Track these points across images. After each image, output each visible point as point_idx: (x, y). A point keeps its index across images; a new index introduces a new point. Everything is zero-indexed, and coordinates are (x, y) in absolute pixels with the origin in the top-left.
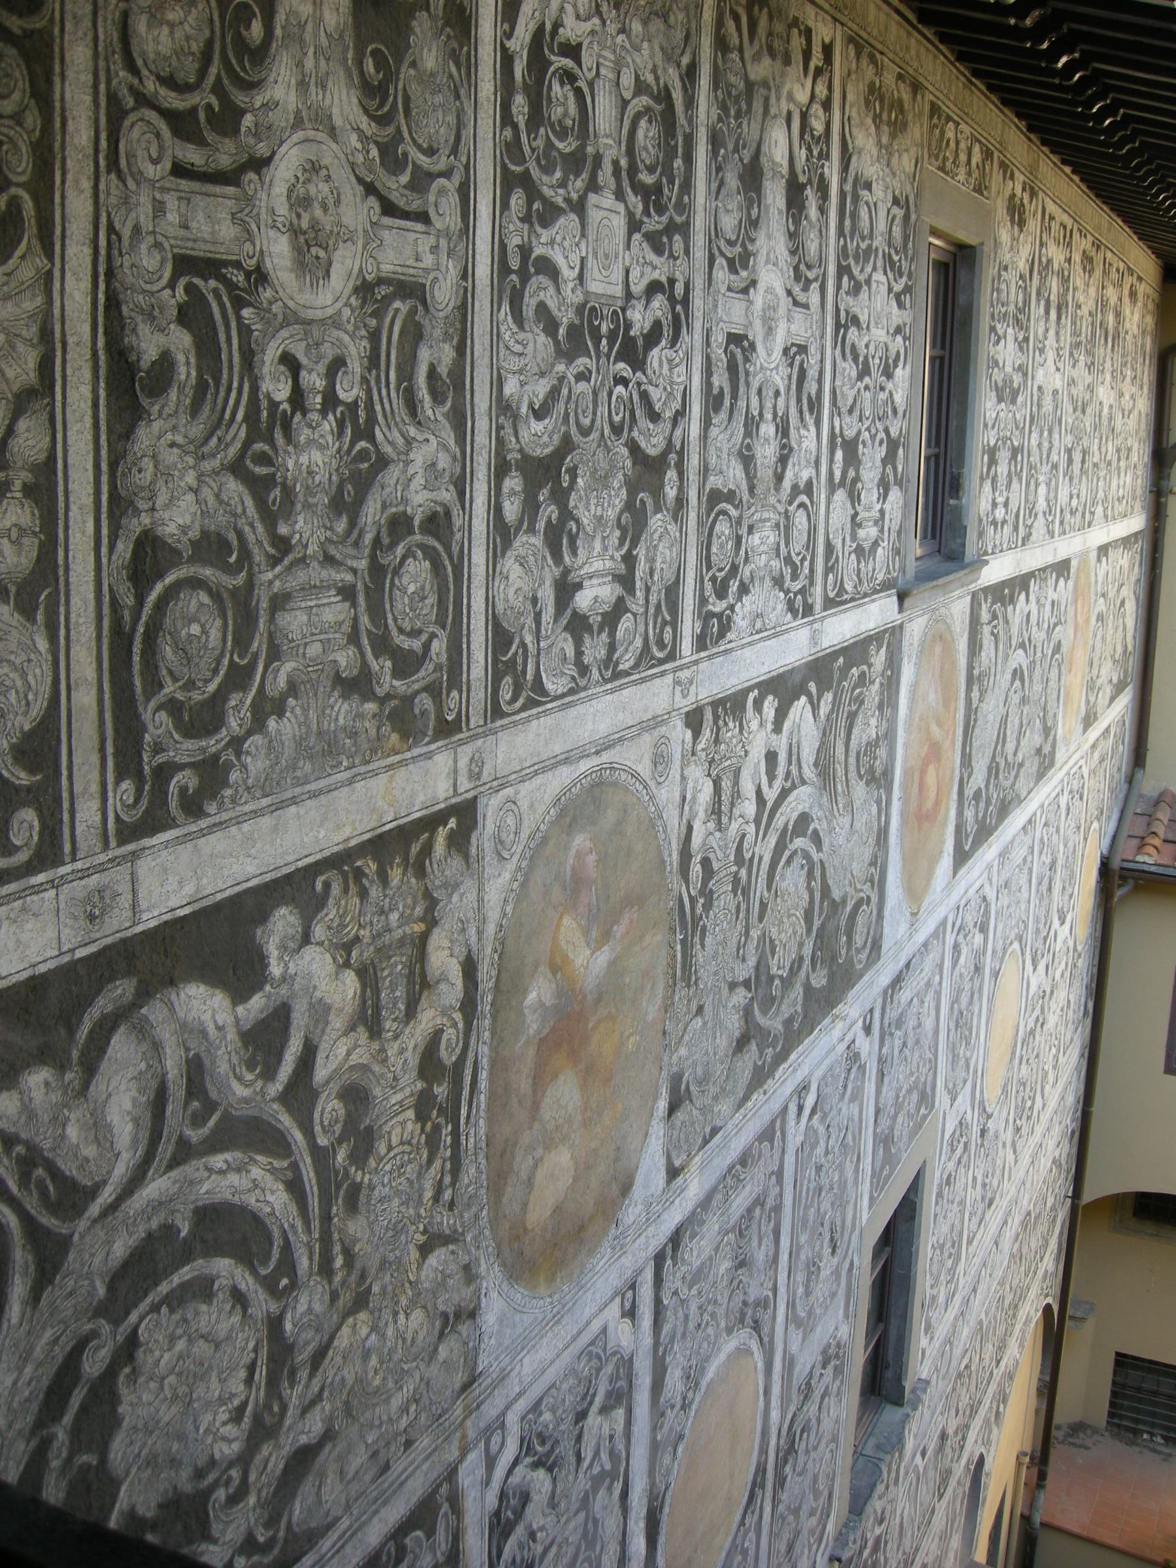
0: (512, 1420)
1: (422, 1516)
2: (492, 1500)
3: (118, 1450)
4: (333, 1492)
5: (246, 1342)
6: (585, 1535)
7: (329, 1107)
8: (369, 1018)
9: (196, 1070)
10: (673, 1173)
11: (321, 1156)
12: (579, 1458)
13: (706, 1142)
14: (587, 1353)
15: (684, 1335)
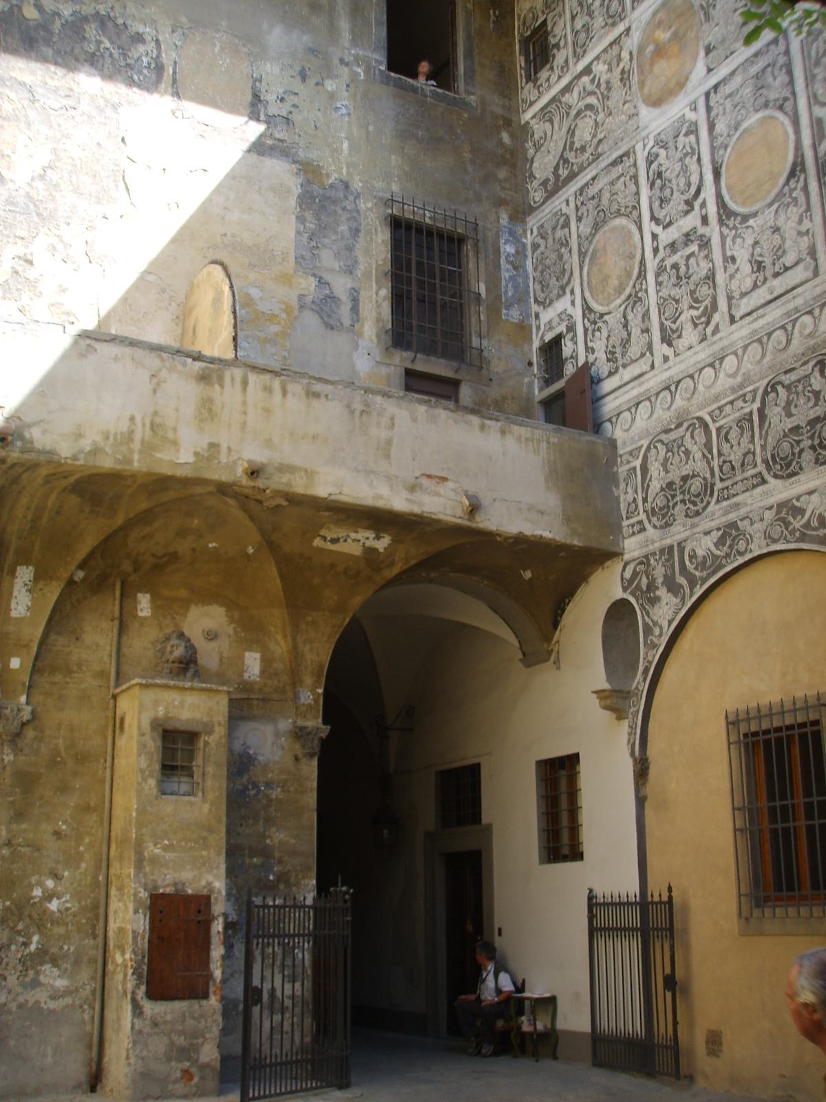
0: (651, 137)
1: (627, 154)
3: (576, 139)
5: (591, 123)
6: (682, 168)
7: (603, 86)
8: (610, 70)
9: (584, 88)
10: (710, 70)
11: (602, 93)
13: (727, 57)
15: (724, 114)
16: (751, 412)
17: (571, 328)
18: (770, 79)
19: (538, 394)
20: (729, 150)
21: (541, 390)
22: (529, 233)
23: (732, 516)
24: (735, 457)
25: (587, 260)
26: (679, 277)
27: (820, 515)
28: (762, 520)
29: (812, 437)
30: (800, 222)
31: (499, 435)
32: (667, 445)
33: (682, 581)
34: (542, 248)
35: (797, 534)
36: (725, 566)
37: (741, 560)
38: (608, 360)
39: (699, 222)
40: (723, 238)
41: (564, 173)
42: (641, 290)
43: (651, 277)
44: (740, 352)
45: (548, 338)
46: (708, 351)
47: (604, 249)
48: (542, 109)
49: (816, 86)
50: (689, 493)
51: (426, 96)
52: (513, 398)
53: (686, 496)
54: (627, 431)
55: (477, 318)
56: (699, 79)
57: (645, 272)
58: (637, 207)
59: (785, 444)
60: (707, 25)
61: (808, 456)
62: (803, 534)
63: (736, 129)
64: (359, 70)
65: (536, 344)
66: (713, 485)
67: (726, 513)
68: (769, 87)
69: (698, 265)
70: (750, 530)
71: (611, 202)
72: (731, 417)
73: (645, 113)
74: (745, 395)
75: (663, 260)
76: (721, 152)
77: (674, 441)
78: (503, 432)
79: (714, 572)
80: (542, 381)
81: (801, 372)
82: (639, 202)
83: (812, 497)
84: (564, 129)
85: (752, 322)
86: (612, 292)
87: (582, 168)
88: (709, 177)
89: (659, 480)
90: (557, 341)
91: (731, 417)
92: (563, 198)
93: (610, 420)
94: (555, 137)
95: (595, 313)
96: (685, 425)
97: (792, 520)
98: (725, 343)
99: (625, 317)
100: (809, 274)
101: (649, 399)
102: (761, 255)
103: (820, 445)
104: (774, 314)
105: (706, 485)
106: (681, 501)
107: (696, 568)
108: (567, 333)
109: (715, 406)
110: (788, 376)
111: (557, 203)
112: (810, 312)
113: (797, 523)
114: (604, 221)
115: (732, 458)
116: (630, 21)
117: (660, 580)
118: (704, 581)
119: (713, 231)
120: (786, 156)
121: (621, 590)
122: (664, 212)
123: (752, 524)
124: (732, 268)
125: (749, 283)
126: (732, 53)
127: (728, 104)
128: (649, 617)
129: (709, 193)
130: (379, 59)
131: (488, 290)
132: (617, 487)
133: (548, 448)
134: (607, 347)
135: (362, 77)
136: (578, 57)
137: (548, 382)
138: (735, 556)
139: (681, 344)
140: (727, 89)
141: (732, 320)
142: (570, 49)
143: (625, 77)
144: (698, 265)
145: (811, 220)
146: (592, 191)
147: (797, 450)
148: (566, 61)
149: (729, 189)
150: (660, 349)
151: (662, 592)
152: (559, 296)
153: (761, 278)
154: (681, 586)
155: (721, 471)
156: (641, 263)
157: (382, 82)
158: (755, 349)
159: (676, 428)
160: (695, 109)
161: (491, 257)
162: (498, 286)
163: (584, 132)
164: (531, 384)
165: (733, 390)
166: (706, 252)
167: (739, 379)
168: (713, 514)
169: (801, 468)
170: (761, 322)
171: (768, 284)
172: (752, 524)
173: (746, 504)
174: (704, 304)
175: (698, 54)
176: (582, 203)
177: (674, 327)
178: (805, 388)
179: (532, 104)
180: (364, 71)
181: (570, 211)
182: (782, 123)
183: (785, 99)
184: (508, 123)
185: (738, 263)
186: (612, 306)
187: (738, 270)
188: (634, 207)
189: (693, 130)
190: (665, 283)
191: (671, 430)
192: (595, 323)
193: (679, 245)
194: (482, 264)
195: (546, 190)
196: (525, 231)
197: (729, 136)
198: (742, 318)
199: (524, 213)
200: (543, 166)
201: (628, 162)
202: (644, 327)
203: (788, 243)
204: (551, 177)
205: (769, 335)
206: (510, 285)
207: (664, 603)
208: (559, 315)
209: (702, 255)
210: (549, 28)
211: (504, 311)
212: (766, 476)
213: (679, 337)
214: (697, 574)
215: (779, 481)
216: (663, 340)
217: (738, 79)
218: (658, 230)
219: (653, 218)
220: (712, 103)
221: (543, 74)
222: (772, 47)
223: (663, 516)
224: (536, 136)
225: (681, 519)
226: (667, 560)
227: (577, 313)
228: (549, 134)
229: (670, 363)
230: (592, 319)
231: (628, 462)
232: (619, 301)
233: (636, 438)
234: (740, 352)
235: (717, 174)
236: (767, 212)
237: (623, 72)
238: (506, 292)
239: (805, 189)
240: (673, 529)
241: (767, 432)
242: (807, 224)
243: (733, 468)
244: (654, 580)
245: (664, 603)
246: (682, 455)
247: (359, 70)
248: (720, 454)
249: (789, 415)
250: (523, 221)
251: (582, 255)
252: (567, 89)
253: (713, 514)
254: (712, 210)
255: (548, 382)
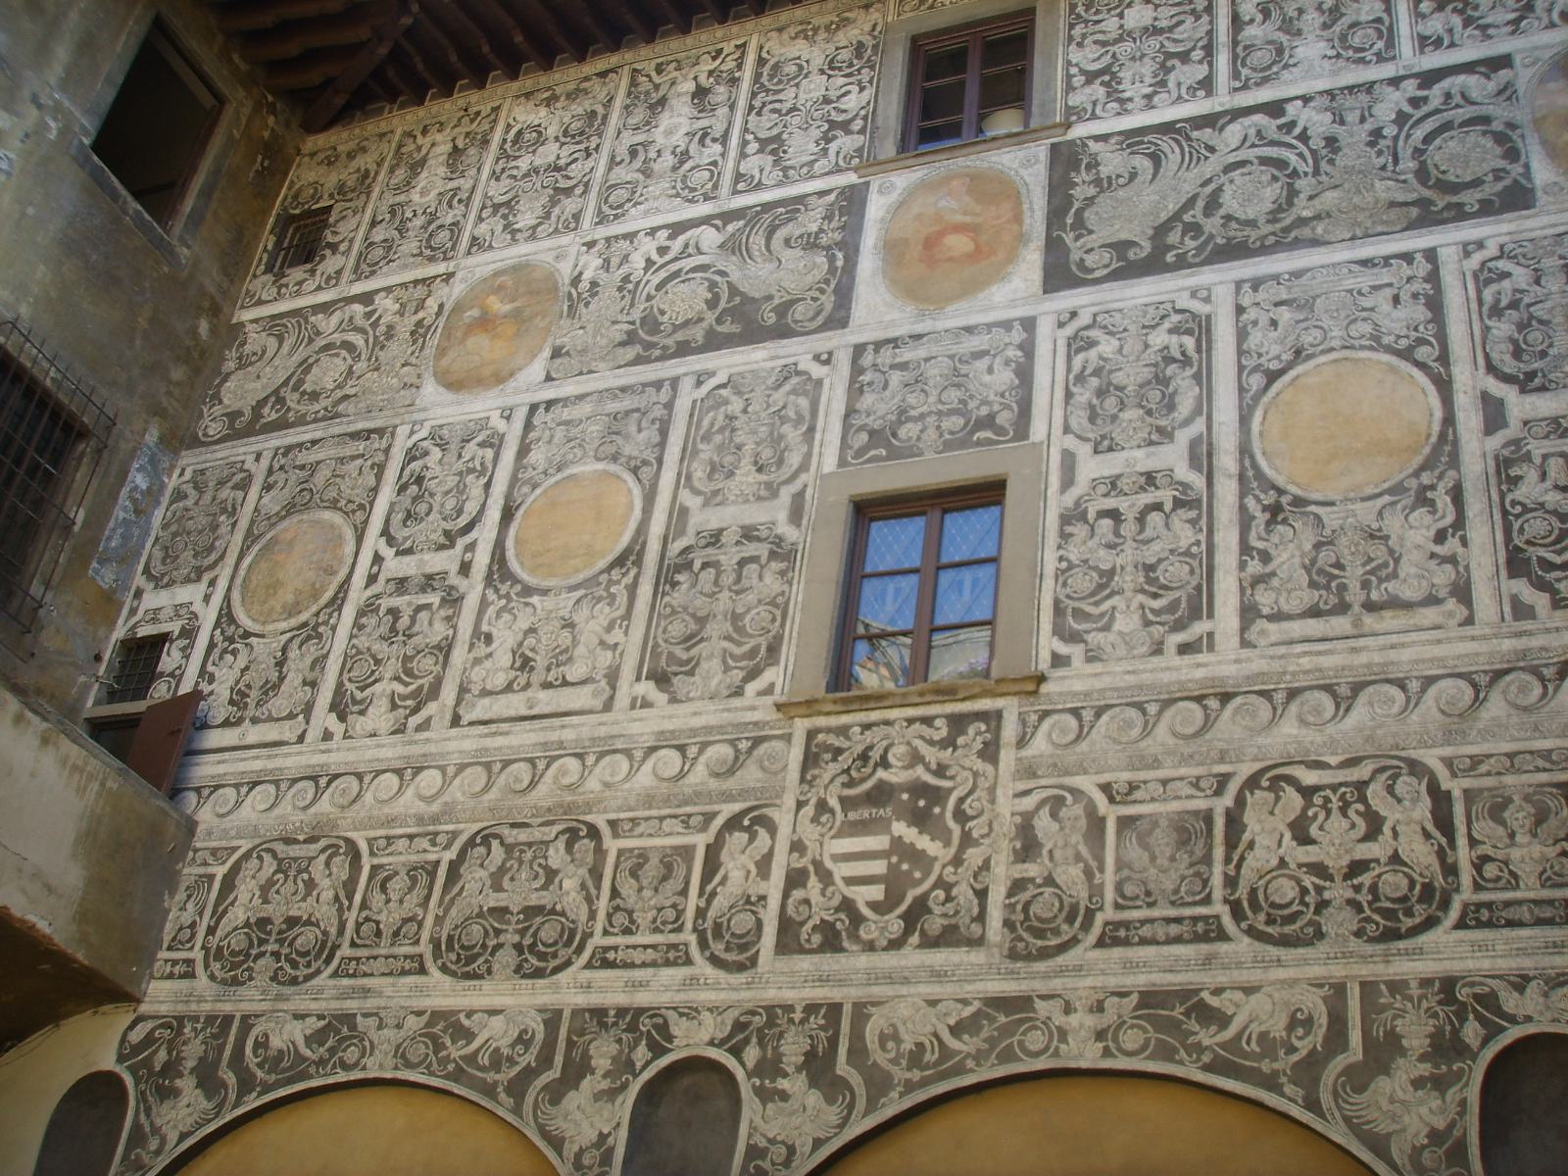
0: (428, 425)
1: (380, 432)
2: (410, 444)
3: (309, 378)
4: (351, 409)
5: (343, 367)
8: (401, 313)
10: (549, 378)
11: (376, 337)
12: (460, 456)
14: (477, 421)
16: (438, 863)
17: (189, 633)
18: (633, 428)
19: (91, 707)
20: (538, 491)
21: (97, 703)
22: (177, 472)
23: (351, 1005)
24: (389, 918)
25: (256, 548)
26: (393, 630)
27: (497, 1050)
28: (399, 1026)
29: (522, 932)
30: (609, 628)
31: (36, 742)
32: (280, 861)
33: (230, 1078)
34: (189, 503)
35: (451, 1067)
36: (311, 1077)
37: (342, 1077)
38: (232, 702)
39: (454, 568)
40: (484, 604)
41: (270, 414)
42: (326, 623)
43: (349, 613)
44: (451, 770)
45: (144, 631)
46: (401, 751)
47: (291, 543)
48: (273, 317)
49: (695, 465)
50: (290, 945)
51: (125, 213)
52: (52, 696)
53: (284, 949)
54: (223, 816)
55: (50, 555)
56: (530, 381)
57: (343, 601)
58: (367, 508)
59: (476, 928)
60: (569, 322)
61: (507, 958)
62: (460, 1070)
63: (559, 470)
64: (52, 124)
65: (120, 632)
66: (335, 947)
67: (343, 996)
68: (627, 437)
69: (431, 624)
70: (374, 1035)
71: (328, 484)
72: (402, 858)
73: (430, 390)
74: (436, 834)
75: (377, 596)
76: (526, 489)
77: (295, 859)
78: (45, 741)
79: (290, 1081)
80: (104, 690)
81: (537, 834)
82: (372, 504)
83: (494, 1019)
84: (297, 358)
85: (486, 736)
86: (278, 608)
87: (302, 421)
88: (494, 514)
89: (248, 909)
90: (159, 642)
91: (402, 858)
92: (254, 448)
93: (198, 790)
94: (276, 362)
95: (238, 626)
96: (323, 843)
97: (448, 1043)
98: (432, 748)
99: (284, 650)
100: (598, 704)
101: (276, 783)
102: (533, 650)
103: (532, 947)
104: (524, 738)
105: (324, 943)
106: (273, 953)
107: (260, 1065)
108: (180, 636)
109: (382, 832)
110: (515, 831)
111: (242, 450)
112: (580, 756)
113: (456, 1051)
114: (306, 507)
115: (382, 917)
116: (457, 266)
117: (190, 1064)
118: (267, 1088)
119: (473, 589)
120: (621, 535)
121: (114, 1058)
122: (406, 532)
123: (380, 1027)
124: (481, 650)
125: (500, 680)
126: (590, 372)
127: (560, 433)
128: (148, 1115)
129: (485, 535)
130: (87, 127)
131: (86, 524)
132: (172, 895)
133: (99, 794)
134: (237, 682)
135: (52, 135)
136: (358, 275)
137: (112, 696)
138: (334, 1067)
139: (361, 724)
140: (566, 414)
141: (456, 721)
142: (352, 261)
143: (420, 331)
144: (431, 624)
145: (626, 633)
146: (303, 458)
147: (491, 943)
148: (339, 273)
149: (517, 542)
150: (323, 717)
151: (187, 1084)
152: (188, 580)
153: (522, 681)
154: (225, 1086)
155: (357, 932)
156: (341, 586)
157: (75, 159)
158: (476, 777)
159: (305, 841)
160: (508, 418)
161: (112, 480)
162: (102, 527)
163: (327, 374)
164: (87, 687)
165: (420, 820)
166: (450, 612)
167: (435, 808)
168: (321, 991)
169: (489, 971)
170: (499, 741)
171: (529, 693)
172: (380, 1027)
173: (380, 994)
174: (420, 681)
175: (540, 350)
176: (282, 468)
177: (359, 695)
178: (535, 857)
179: (260, 303)
180: (59, 129)
181: (259, 471)
182: (630, 491)
183: (645, 463)
184: (215, 311)
185: (494, 645)
186: (270, 627)
187: (490, 655)
188: (361, 507)
189: (495, 443)
190: (368, 630)
191: (296, 841)
192: (231, 640)
193: (411, 585)
194: (95, 483)
195: (231, 426)
196: (172, 467)
197: (545, 473)
198: (471, 724)
199: (182, 442)
200: (240, 391)
201: (377, 443)
202: (310, 677)
203: (581, 650)
204: (248, 412)
205: (506, 764)
206: (120, 531)
207: (185, 1102)
208: (177, 607)
209: (443, 613)
210: (331, 220)
211: (95, 565)
212: (429, 963)
213: (362, 713)
214: (260, 1074)
215: (447, 978)
216: (333, 707)
217: (586, 408)
218: (388, 553)
219: (385, 532)
220: (536, 421)
221: (297, 274)
222: (651, 390)
223: (234, 966)
224: (248, 349)
225: (262, 980)
226: (214, 1036)
227: (209, 616)
228: (270, 353)
229: (332, 745)
230: (229, 633)
231: (205, 864)
232: (284, 625)
233: (233, 833)
234: (451, 770)
235: (508, 514)
236: (564, 596)
237: (419, 324)
238: (110, 538)
239: (632, 590)
240: (242, 990)
241: (452, 900)
242: (617, 635)
243: (378, 933)
244: (179, 1060)
245: (185, 1102)
246: (301, 885)
247: (52, 124)
248: (364, 906)
249: (498, 888)
250: (176, 452)
251: (250, 538)
252: (325, 308)
253: (321, 991)
254: (482, 559)
255: (112, 696)
